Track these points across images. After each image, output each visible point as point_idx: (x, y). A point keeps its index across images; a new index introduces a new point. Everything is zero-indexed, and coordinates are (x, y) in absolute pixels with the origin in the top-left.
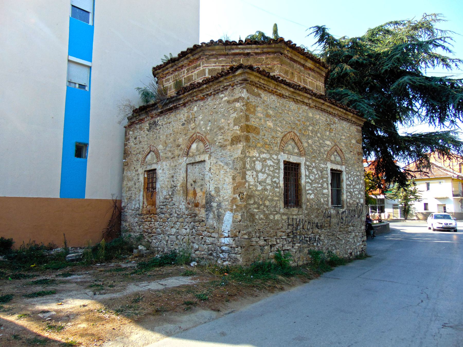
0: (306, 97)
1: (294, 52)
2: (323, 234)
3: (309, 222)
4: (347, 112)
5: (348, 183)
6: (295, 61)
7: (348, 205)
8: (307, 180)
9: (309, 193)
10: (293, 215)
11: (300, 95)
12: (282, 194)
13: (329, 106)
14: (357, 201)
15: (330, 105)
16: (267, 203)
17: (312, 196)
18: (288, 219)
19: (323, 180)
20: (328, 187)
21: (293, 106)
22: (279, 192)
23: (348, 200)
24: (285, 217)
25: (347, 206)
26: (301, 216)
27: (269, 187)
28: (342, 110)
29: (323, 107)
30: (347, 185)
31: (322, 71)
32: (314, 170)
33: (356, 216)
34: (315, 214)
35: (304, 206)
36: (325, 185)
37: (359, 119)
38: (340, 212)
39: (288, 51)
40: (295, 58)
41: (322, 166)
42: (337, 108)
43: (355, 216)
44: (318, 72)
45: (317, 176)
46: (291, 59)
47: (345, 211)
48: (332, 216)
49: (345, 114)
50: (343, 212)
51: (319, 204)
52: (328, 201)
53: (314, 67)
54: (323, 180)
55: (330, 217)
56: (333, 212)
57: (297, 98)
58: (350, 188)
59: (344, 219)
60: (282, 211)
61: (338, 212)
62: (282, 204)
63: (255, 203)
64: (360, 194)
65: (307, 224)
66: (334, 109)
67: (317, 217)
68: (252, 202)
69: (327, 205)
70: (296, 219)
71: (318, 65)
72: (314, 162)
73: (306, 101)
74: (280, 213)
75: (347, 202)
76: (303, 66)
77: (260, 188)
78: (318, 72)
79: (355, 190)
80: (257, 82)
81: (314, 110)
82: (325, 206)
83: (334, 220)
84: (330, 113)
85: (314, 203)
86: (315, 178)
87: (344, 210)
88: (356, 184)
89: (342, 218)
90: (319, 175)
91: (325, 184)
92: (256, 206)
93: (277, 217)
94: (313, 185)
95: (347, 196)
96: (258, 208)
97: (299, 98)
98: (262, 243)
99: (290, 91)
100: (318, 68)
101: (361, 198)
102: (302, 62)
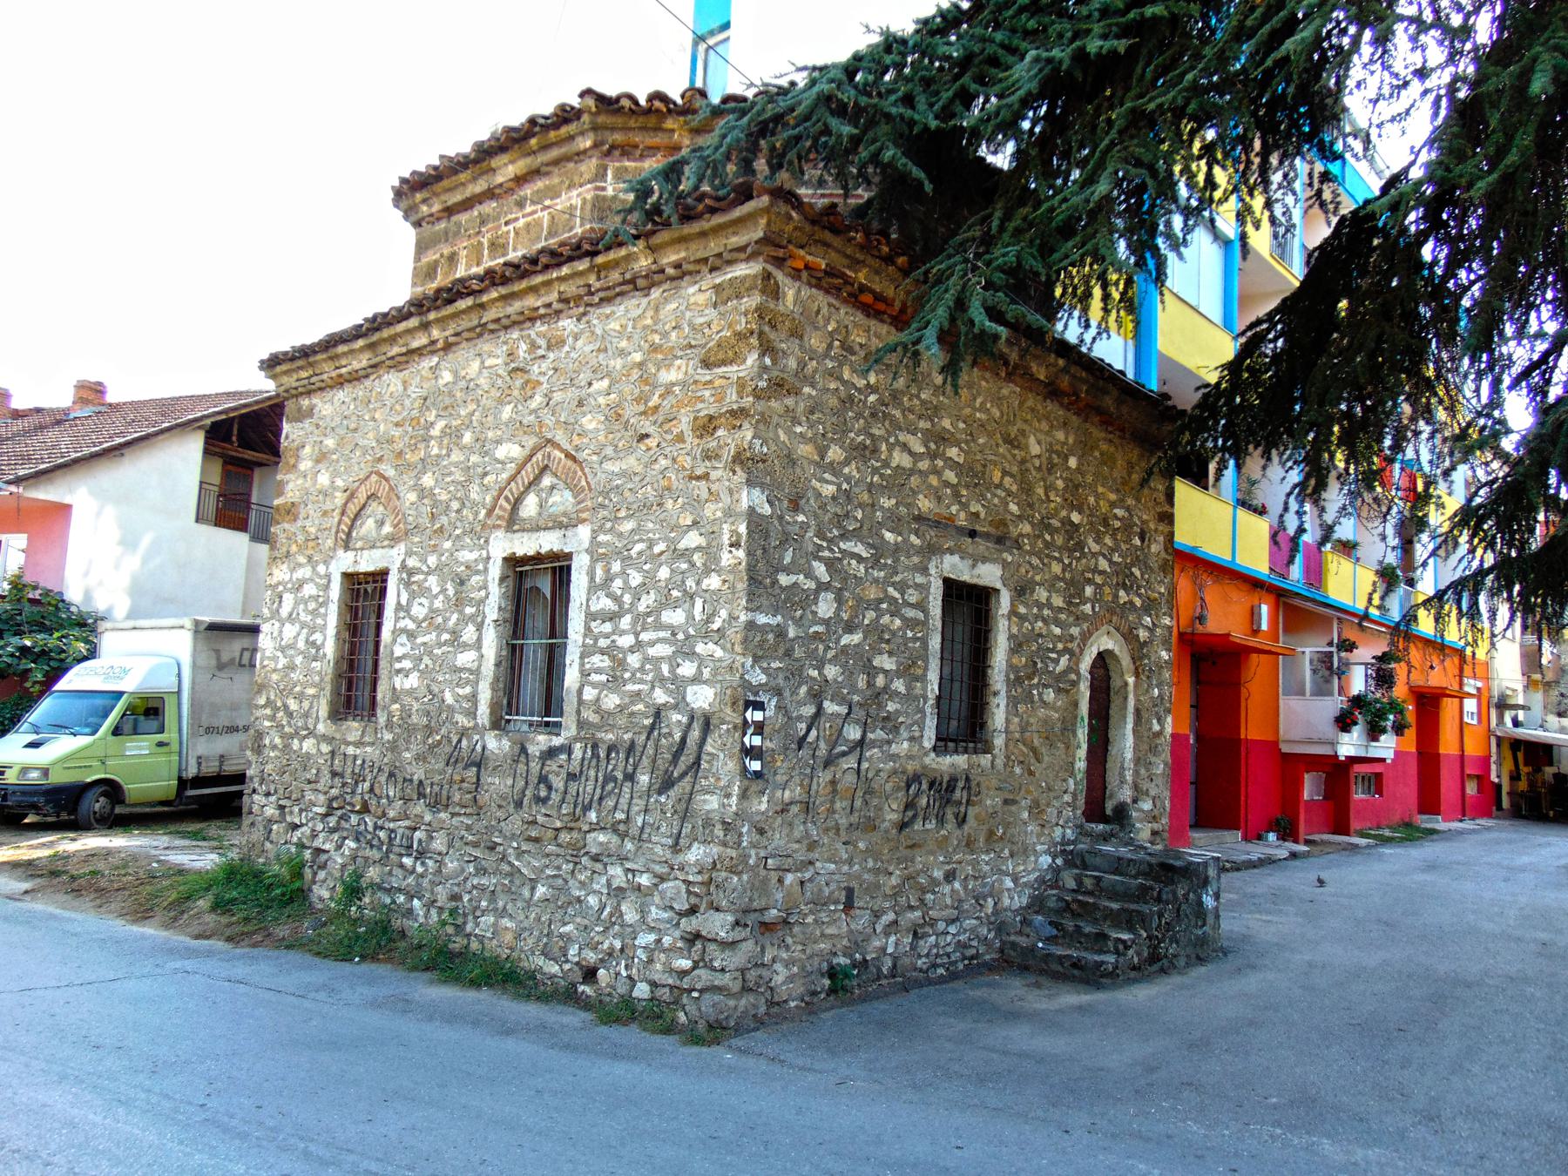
0: (409, 331)
1: (438, 187)
2: (442, 832)
3: (391, 775)
4: (600, 260)
5: (603, 603)
6: (467, 205)
7: (589, 715)
8: (401, 624)
9: (399, 671)
10: (348, 744)
11: (392, 340)
12: (328, 679)
13: (503, 298)
14: (660, 697)
15: (503, 290)
16: (293, 705)
17: (413, 681)
18: (333, 753)
19: (461, 612)
20: (479, 640)
21: (392, 381)
22: (320, 673)
23: (589, 694)
24: (325, 748)
25: (581, 724)
26: (368, 749)
27: (299, 660)
28: (565, 270)
29: (491, 314)
30: (591, 616)
31: (571, 138)
32: (433, 582)
33: (644, 779)
34: (415, 748)
35: (382, 718)
36: (469, 634)
37: (703, 234)
38: (534, 750)
39: (424, 201)
40: (457, 197)
41: (467, 556)
42: (539, 279)
43: (630, 777)
44: (556, 162)
45: (438, 604)
46: (449, 211)
47: (568, 749)
48: (491, 765)
49: (599, 270)
50: (551, 753)
51: (437, 713)
52: (473, 698)
53: (528, 160)
54: (461, 612)
55: (478, 765)
56: (495, 744)
57: (390, 354)
58: (618, 631)
59: (558, 782)
60: (321, 728)
61: (523, 750)
62: (323, 709)
63: (269, 703)
64: (692, 655)
65: (383, 778)
66: (533, 290)
67: (420, 758)
68: (262, 701)
69: (472, 714)
70: (355, 757)
71: (533, 141)
72: (435, 549)
73: (420, 341)
74: (315, 736)
75: (580, 702)
76: (490, 194)
77: (282, 662)
78: (556, 162)
79: (644, 637)
80: (295, 384)
81: (462, 353)
82: (462, 720)
83: (497, 784)
84: (531, 318)
85: (416, 706)
86: (432, 610)
87: (557, 741)
88: (666, 603)
89: (543, 779)
90: (447, 598)
91: (471, 628)
92: (268, 711)
93: (308, 745)
94: (419, 640)
95: (585, 674)
96: (273, 718)
97: (396, 350)
98: (270, 811)
99: (362, 350)
100: (545, 147)
101: (697, 679)
102: (479, 187)
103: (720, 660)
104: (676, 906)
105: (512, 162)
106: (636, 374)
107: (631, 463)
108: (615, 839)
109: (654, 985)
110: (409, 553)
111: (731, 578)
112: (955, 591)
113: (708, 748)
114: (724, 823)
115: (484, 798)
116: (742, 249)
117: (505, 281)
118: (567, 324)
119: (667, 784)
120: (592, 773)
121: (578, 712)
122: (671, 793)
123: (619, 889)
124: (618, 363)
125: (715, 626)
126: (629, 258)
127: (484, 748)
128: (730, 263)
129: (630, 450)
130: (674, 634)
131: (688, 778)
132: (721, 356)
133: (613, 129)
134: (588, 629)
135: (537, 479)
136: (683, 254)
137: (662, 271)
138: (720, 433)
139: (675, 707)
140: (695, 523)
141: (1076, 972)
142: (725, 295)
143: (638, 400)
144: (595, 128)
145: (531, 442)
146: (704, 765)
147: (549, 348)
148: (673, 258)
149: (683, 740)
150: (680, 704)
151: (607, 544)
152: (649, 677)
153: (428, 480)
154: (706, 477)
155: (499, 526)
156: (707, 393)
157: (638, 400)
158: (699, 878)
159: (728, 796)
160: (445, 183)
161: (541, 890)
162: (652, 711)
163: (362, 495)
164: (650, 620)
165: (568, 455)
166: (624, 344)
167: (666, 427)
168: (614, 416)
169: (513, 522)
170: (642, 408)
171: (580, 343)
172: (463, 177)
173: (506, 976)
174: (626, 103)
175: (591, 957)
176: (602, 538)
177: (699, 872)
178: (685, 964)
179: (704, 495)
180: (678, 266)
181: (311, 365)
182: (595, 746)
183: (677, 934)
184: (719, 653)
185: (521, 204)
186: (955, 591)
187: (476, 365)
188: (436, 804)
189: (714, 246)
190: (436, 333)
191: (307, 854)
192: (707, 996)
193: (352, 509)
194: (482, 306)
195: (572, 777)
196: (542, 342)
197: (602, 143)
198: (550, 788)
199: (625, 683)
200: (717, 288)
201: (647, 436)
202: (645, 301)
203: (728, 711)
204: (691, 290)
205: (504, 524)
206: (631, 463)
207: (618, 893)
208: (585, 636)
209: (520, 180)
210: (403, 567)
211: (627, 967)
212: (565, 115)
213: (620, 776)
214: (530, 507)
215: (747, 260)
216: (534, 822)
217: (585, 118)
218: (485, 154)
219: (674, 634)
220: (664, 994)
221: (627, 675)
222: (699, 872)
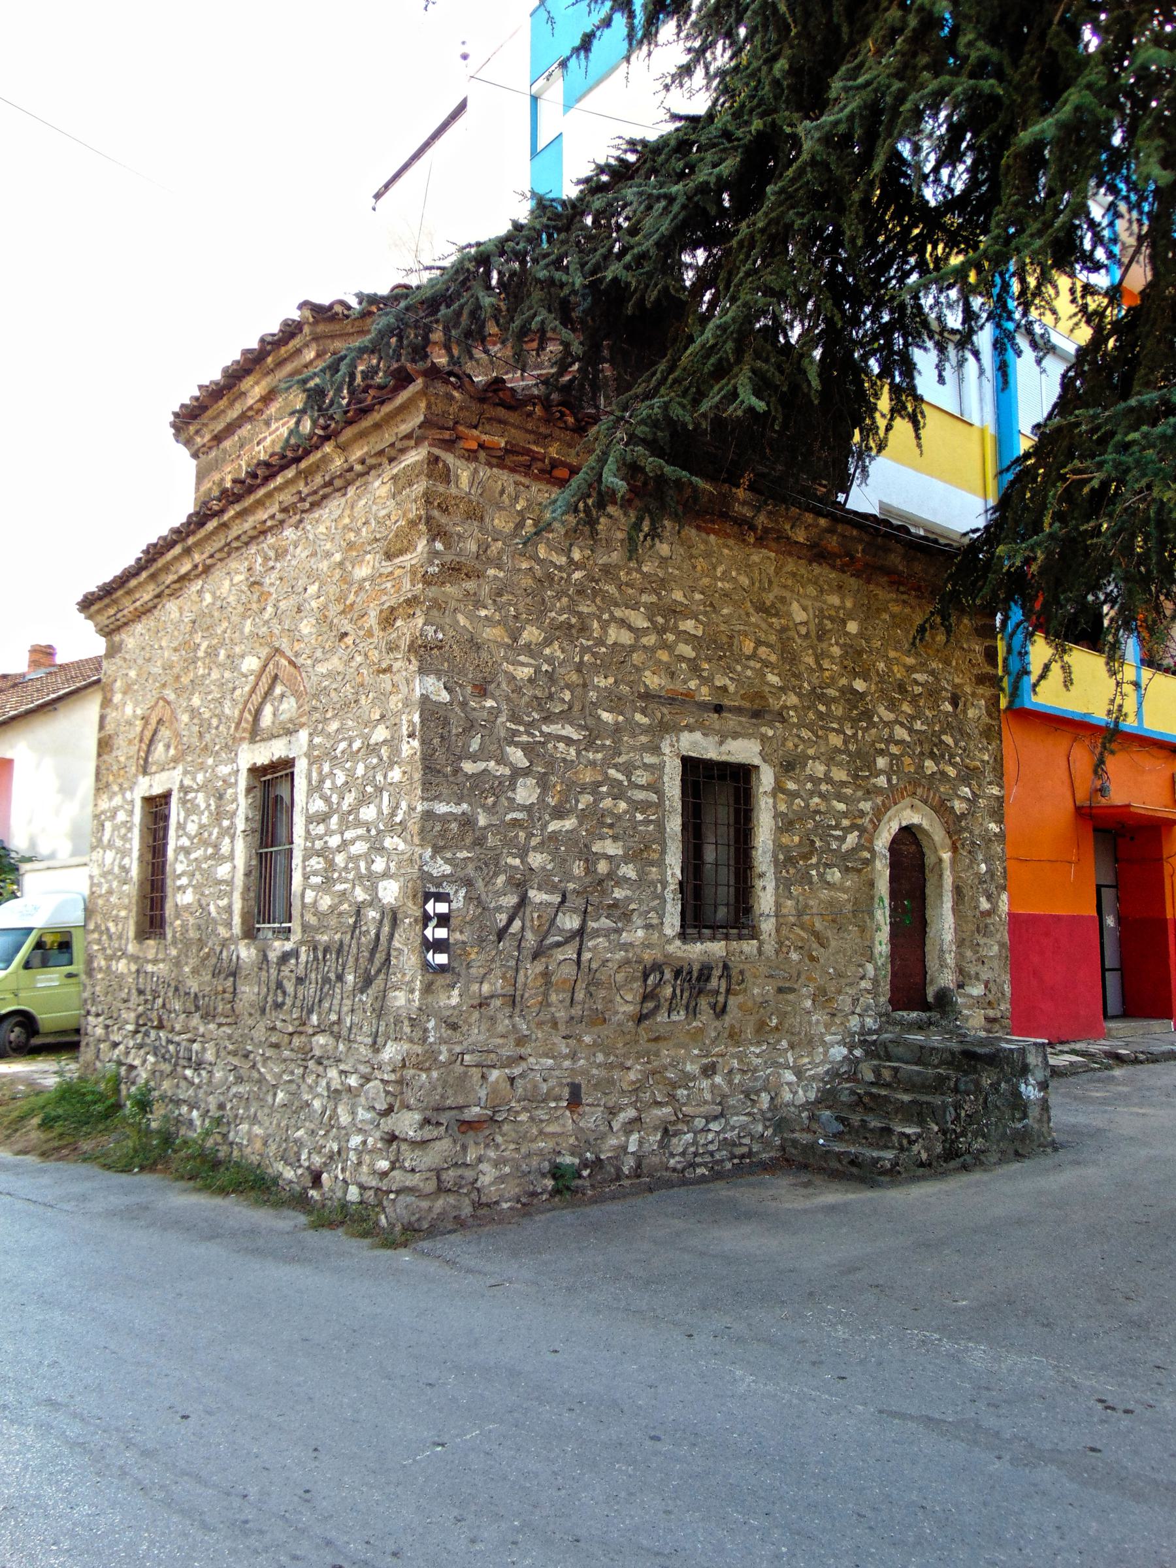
0: (176, 559)
1: (205, 418)
2: (210, 1040)
3: (177, 989)
4: (303, 465)
5: (318, 805)
6: (230, 429)
7: (313, 920)
8: (180, 843)
9: (179, 888)
10: (148, 961)
11: (166, 568)
12: (134, 901)
14: (360, 895)
15: (238, 507)
18: (138, 971)
20: (232, 850)
21: (171, 607)
23: (310, 896)
24: (133, 968)
25: (305, 927)
26: (161, 966)
28: (279, 480)
29: (234, 532)
30: (310, 820)
31: (298, 351)
32: (201, 799)
33: (350, 978)
34: (193, 962)
36: (225, 848)
37: (377, 426)
38: (273, 956)
39: (197, 432)
40: (219, 426)
41: (224, 770)
42: (261, 492)
43: (340, 978)
45: (205, 820)
46: (218, 439)
47: (295, 953)
48: (244, 973)
49: (307, 475)
50: (285, 958)
51: (206, 925)
52: (229, 909)
53: (269, 379)
54: (220, 826)
55: (234, 974)
56: (246, 953)
57: (168, 582)
58: (329, 833)
61: (265, 956)
63: (97, 927)
64: (381, 850)
66: (260, 503)
67: (195, 971)
69: (229, 925)
71: (270, 360)
72: (202, 767)
73: (185, 567)
75: (304, 905)
76: (244, 418)
79: (348, 835)
80: (107, 622)
81: (218, 574)
82: (223, 932)
83: (249, 992)
84: (263, 531)
85: (192, 921)
86: (202, 826)
87: (289, 946)
88: (364, 800)
89: (280, 985)
90: (211, 813)
91: (227, 840)
93: (121, 966)
94: (193, 856)
95: (306, 877)
98: (99, 1031)
99: (146, 582)
100: (280, 364)
101: (386, 875)
102: (233, 414)
103: (403, 853)
104: (378, 1107)
105: (257, 383)
106: (337, 573)
107: (335, 663)
108: (331, 1041)
109: (362, 1188)
110: (185, 772)
111: (408, 769)
112: (696, 771)
113: (396, 944)
114: (410, 1019)
115: (239, 1006)
116: (408, 437)
117: (238, 498)
118: (289, 533)
119: (367, 982)
120: (313, 976)
121: (302, 916)
122: (370, 991)
123: (336, 1091)
124: (324, 565)
125: (398, 819)
126: (326, 459)
127: (238, 957)
128: (403, 451)
129: (333, 650)
130: (368, 831)
131: (382, 976)
132: (398, 546)
133: (332, 337)
134: (308, 832)
135: (271, 688)
136: (365, 449)
137: (351, 469)
138: (399, 623)
139: (371, 904)
140: (383, 717)
141: (854, 1170)
142: (400, 483)
143: (338, 600)
144: (316, 338)
145: (264, 652)
146: (393, 961)
147: (276, 560)
148: (359, 454)
149: (378, 936)
150: (374, 901)
151: (320, 745)
152: (351, 876)
153: (196, 701)
154: (388, 670)
155: (242, 739)
156: (389, 585)
157: (338, 600)
158: (392, 1077)
159: (412, 991)
160: (210, 413)
161: (280, 1095)
162: (354, 909)
163: (153, 721)
164: (351, 818)
165: (291, 663)
166: (328, 546)
167: (360, 623)
168: (323, 619)
169: (255, 734)
170: (341, 607)
171: (298, 550)
172: (222, 403)
173: (256, 1185)
174: (338, 309)
175: (317, 1160)
176: (317, 740)
177: (393, 1071)
178: (384, 1165)
179: (389, 688)
180: (362, 462)
181: (115, 602)
182: (315, 949)
183: (378, 1134)
184: (402, 846)
185: (268, 423)
186: (696, 771)
187: (227, 583)
188: (208, 1016)
189: (388, 437)
190: (197, 557)
191: (123, 1070)
192: (401, 1197)
193: (148, 734)
194: (225, 526)
195: (300, 981)
196: (272, 554)
197: (324, 352)
198: (284, 993)
199: (335, 881)
200: (394, 478)
201: (346, 634)
202: (343, 500)
203: (410, 904)
204: (377, 484)
205: (247, 735)
206: (335, 663)
207: (335, 1095)
208: (306, 839)
209: (267, 399)
210: (182, 786)
211: (343, 1170)
212: (290, 330)
213: (332, 976)
214: (266, 719)
215: (417, 445)
216: (274, 1029)
217: (306, 329)
218: (236, 376)
219: (368, 831)
220: (370, 1195)
221: (336, 875)
222: (393, 1071)
